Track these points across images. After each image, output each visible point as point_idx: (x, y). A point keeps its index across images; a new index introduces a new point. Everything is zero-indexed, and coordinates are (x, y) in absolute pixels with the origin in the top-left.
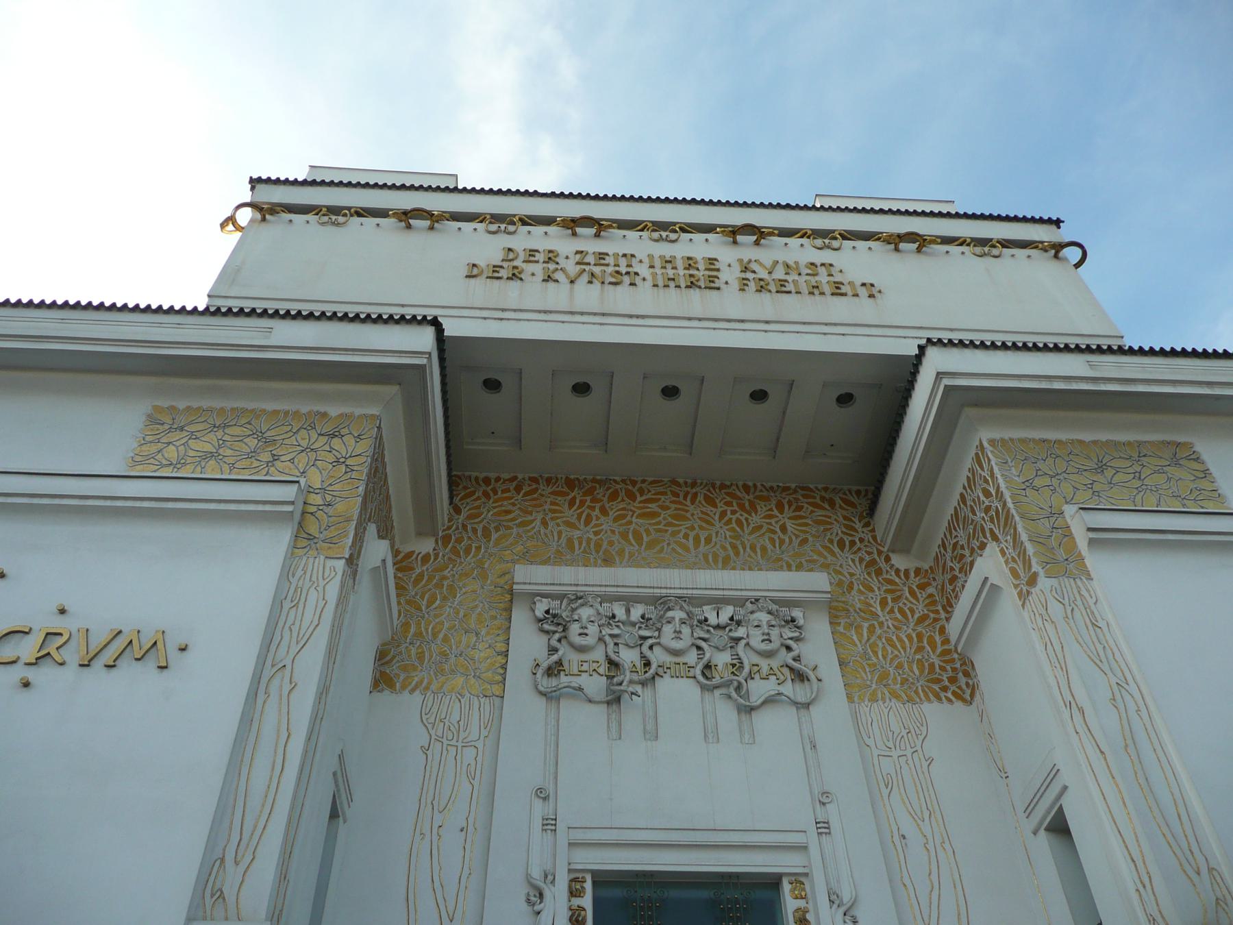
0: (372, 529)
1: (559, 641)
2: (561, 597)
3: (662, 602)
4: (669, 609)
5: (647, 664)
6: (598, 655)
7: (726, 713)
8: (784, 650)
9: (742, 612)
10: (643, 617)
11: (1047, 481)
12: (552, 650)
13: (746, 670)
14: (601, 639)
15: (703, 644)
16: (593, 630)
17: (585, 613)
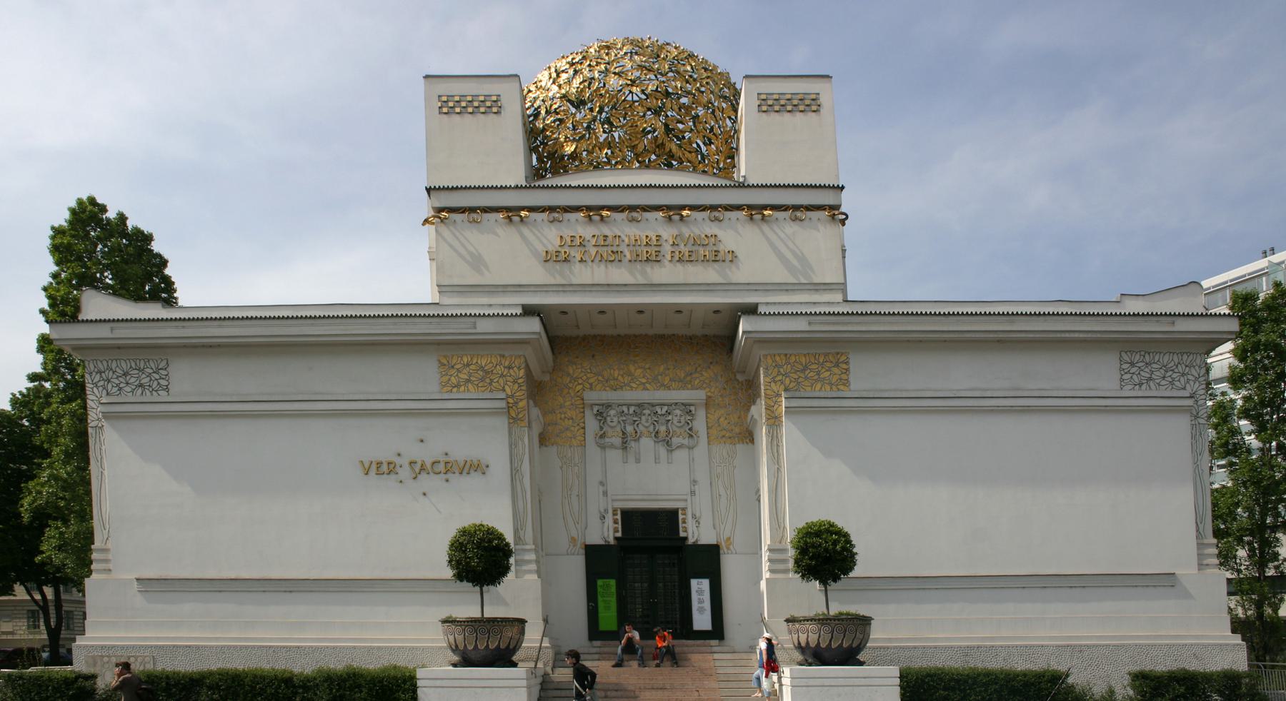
0: (531, 402)
1: (603, 423)
2: (603, 405)
3: (640, 405)
4: (644, 410)
5: (636, 432)
6: (618, 429)
7: (662, 450)
8: (686, 424)
9: (671, 408)
10: (634, 411)
11: (780, 378)
12: (601, 428)
13: (671, 434)
14: (619, 422)
15: (655, 423)
16: (615, 419)
17: (612, 412)
